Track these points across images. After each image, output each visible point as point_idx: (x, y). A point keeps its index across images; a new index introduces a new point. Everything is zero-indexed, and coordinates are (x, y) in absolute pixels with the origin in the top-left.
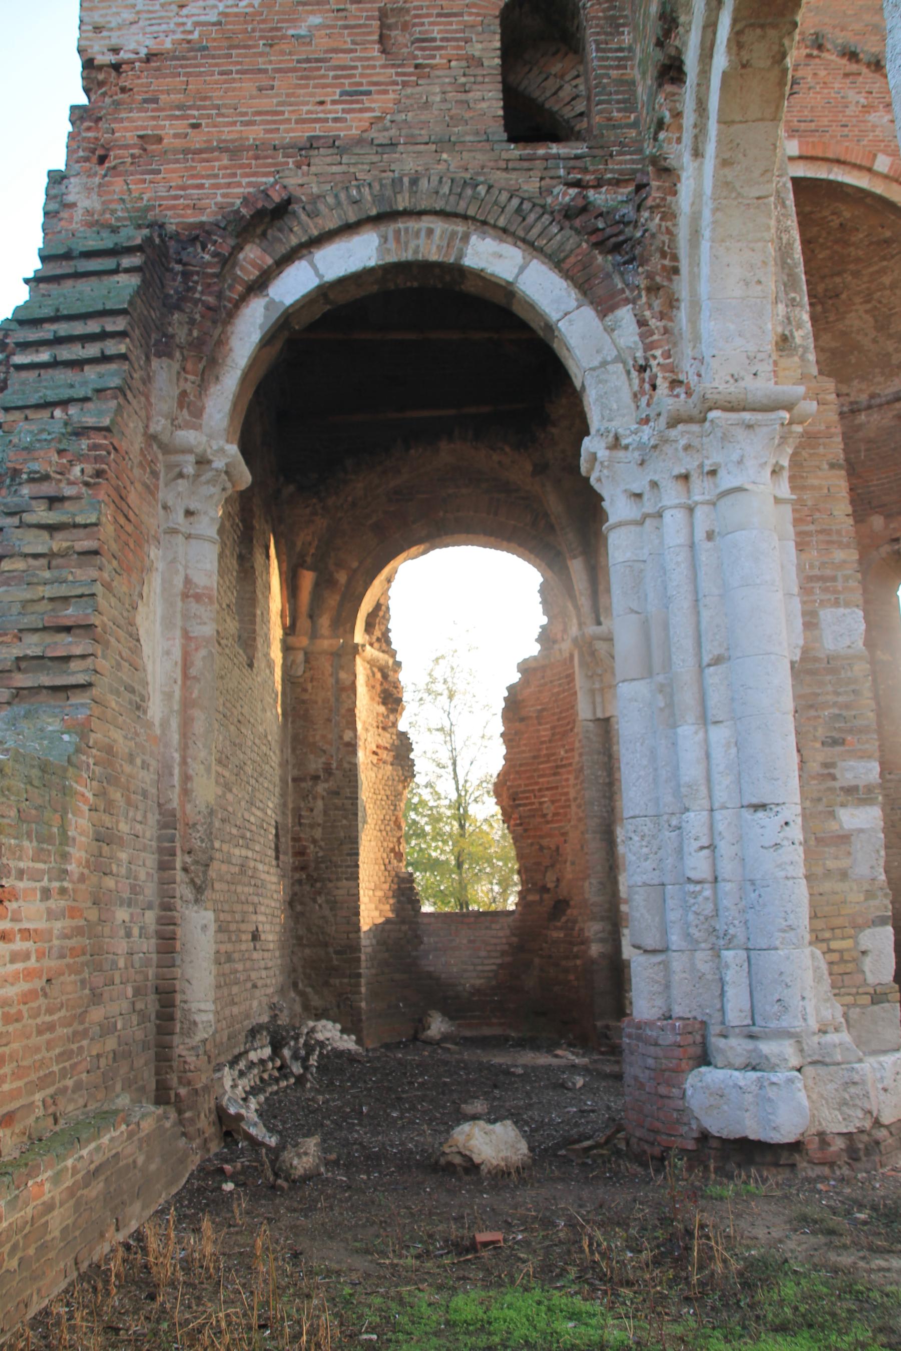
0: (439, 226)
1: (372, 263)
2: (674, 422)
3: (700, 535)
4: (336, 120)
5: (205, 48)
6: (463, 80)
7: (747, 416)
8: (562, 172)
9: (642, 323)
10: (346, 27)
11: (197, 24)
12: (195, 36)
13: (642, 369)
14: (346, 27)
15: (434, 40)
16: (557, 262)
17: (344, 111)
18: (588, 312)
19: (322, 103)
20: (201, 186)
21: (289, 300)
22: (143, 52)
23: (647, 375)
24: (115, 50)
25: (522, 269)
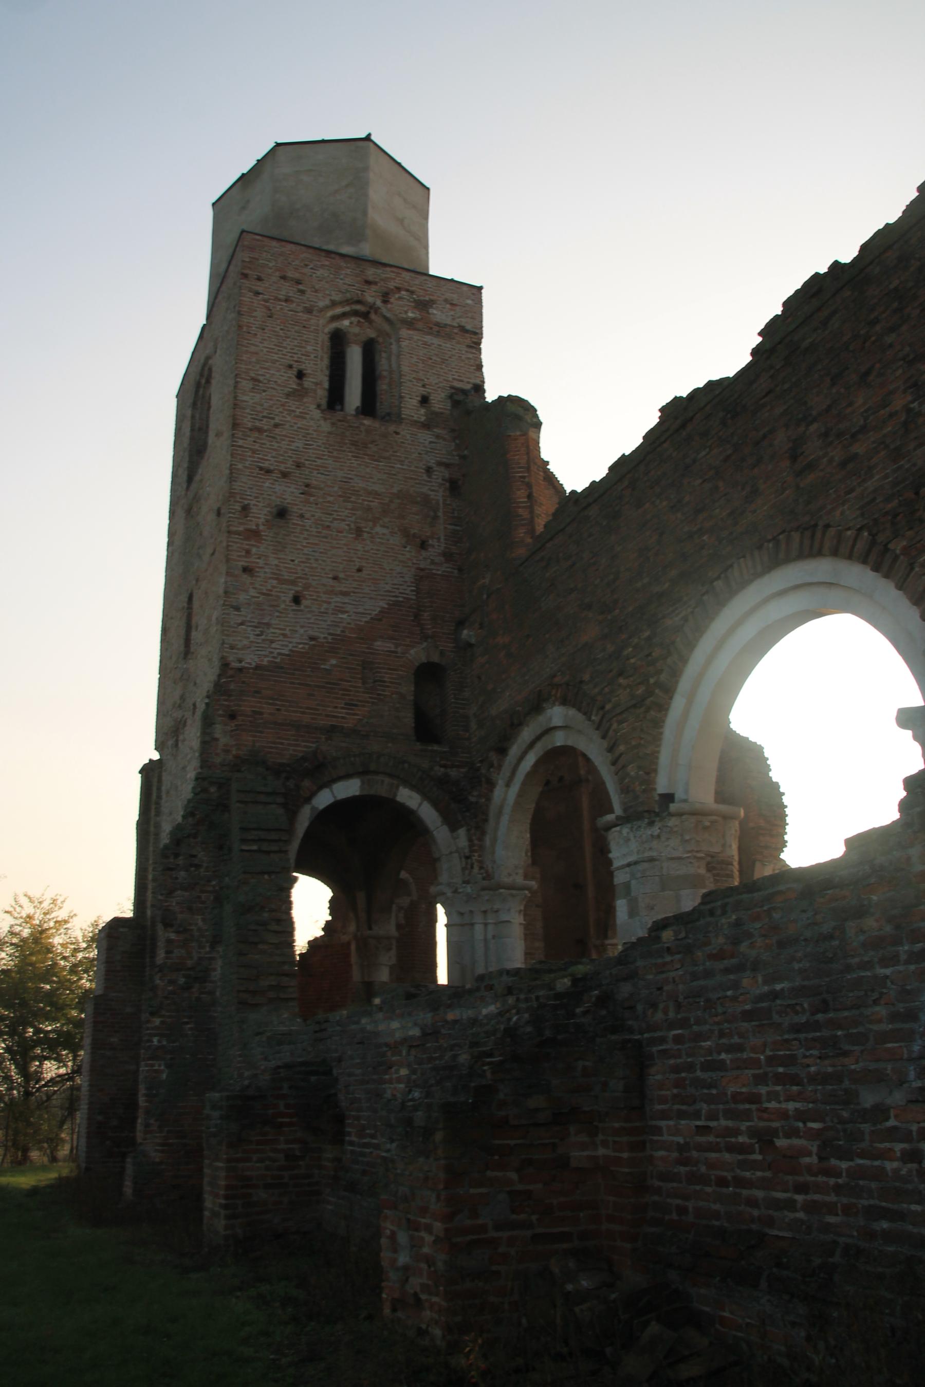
0: (387, 780)
1: (357, 793)
2: (483, 889)
3: (490, 936)
4: (343, 718)
5: (282, 668)
6: (398, 705)
7: (514, 892)
8: (438, 759)
9: (470, 840)
10: (348, 668)
11: (279, 654)
12: (278, 660)
13: (467, 858)
14: (348, 668)
15: (384, 682)
16: (435, 804)
17: (347, 713)
18: (445, 828)
19: (336, 707)
20: (282, 744)
21: (321, 807)
22: (254, 664)
23: (469, 861)
24: (240, 661)
25: (420, 805)
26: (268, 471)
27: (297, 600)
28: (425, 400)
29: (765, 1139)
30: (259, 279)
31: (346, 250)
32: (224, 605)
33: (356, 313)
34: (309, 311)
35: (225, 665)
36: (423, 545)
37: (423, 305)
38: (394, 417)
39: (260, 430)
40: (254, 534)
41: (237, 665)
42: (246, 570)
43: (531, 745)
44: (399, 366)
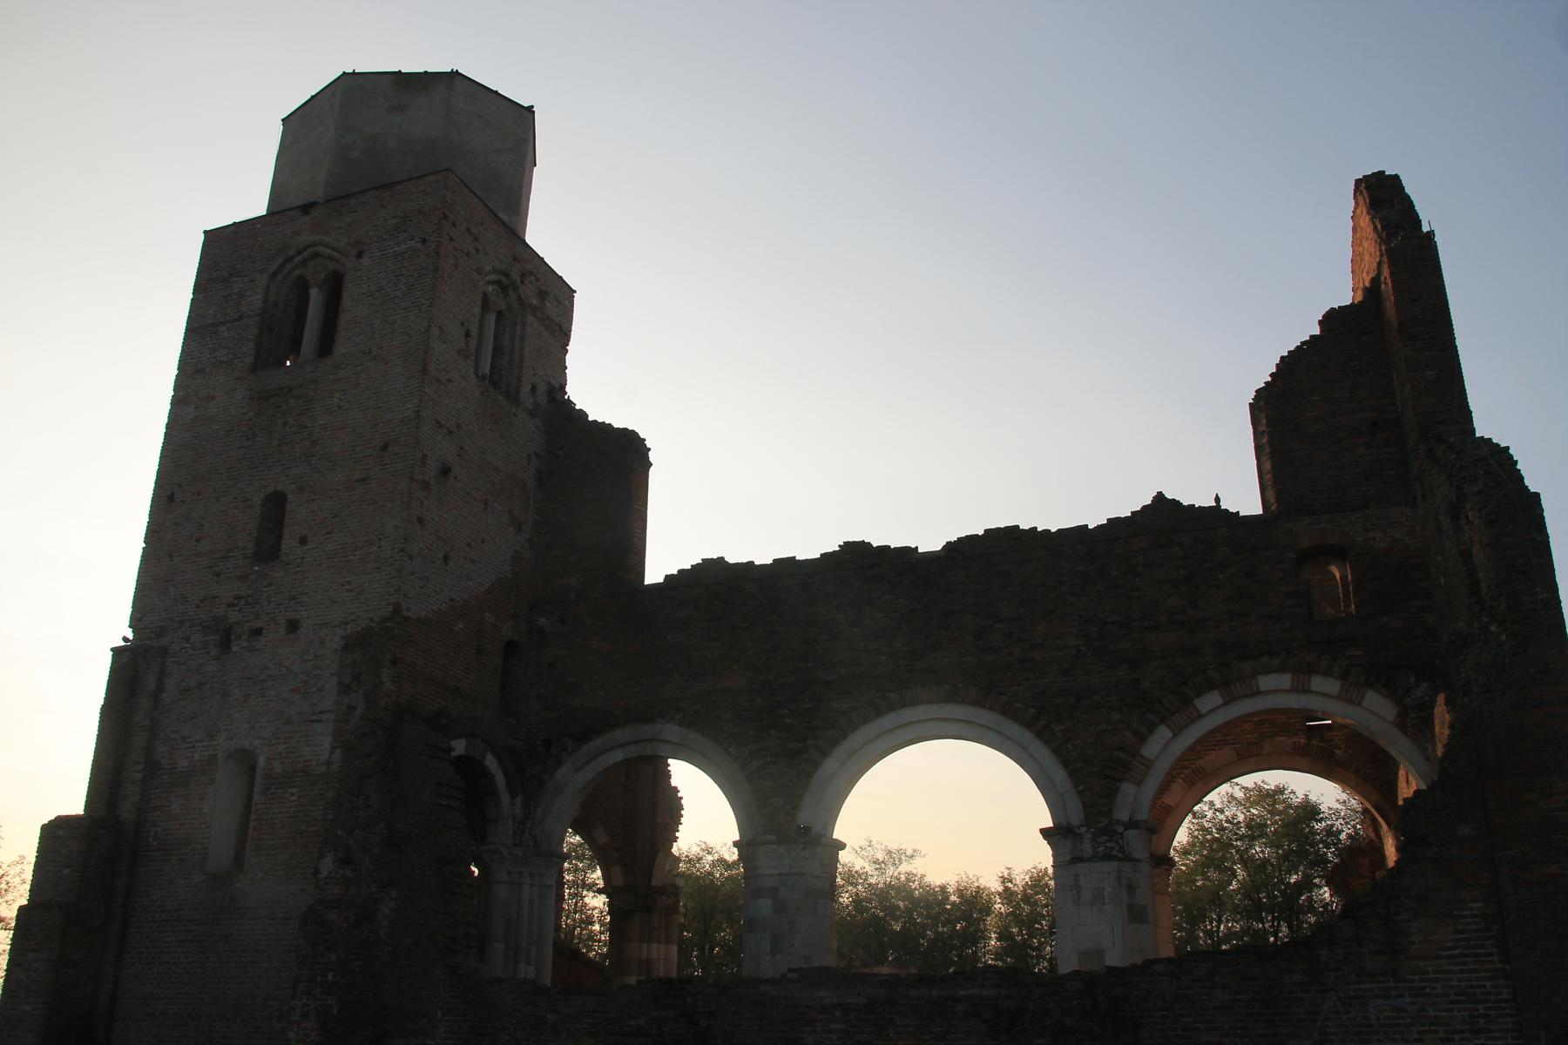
26: (441, 426)
27: (446, 559)
28: (533, 389)
30: (454, 225)
31: (501, 215)
32: (402, 550)
33: (498, 283)
34: (479, 271)
35: (397, 611)
36: (519, 529)
37: (542, 295)
38: (513, 397)
39: (437, 380)
40: (426, 486)
41: (405, 613)
42: (420, 521)
43: (623, 746)
44: (522, 349)
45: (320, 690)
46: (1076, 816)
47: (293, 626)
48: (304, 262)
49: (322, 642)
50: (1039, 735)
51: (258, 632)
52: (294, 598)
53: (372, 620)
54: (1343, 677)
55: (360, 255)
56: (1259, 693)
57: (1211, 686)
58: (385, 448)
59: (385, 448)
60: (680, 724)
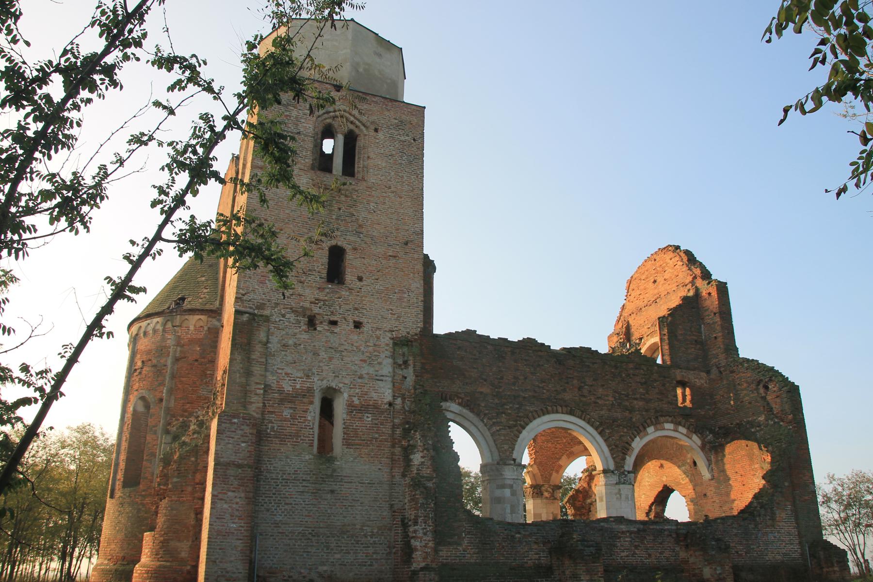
29: (737, 552)
45: (380, 363)
46: (612, 467)
47: (358, 325)
48: (334, 117)
49: (378, 338)
50: (600, 433)
51: (334, 323)
52: (356, 309)
53: (408, 333)
54: (688, 428)
55: (376, 130)
56: (664, 429)
57: (652, 424)
58: (406, 244)
59: (406, 244)
60: (460, 404)
